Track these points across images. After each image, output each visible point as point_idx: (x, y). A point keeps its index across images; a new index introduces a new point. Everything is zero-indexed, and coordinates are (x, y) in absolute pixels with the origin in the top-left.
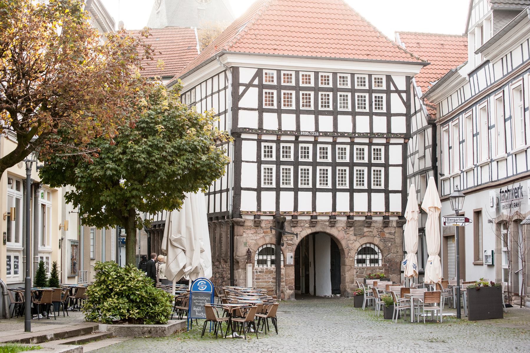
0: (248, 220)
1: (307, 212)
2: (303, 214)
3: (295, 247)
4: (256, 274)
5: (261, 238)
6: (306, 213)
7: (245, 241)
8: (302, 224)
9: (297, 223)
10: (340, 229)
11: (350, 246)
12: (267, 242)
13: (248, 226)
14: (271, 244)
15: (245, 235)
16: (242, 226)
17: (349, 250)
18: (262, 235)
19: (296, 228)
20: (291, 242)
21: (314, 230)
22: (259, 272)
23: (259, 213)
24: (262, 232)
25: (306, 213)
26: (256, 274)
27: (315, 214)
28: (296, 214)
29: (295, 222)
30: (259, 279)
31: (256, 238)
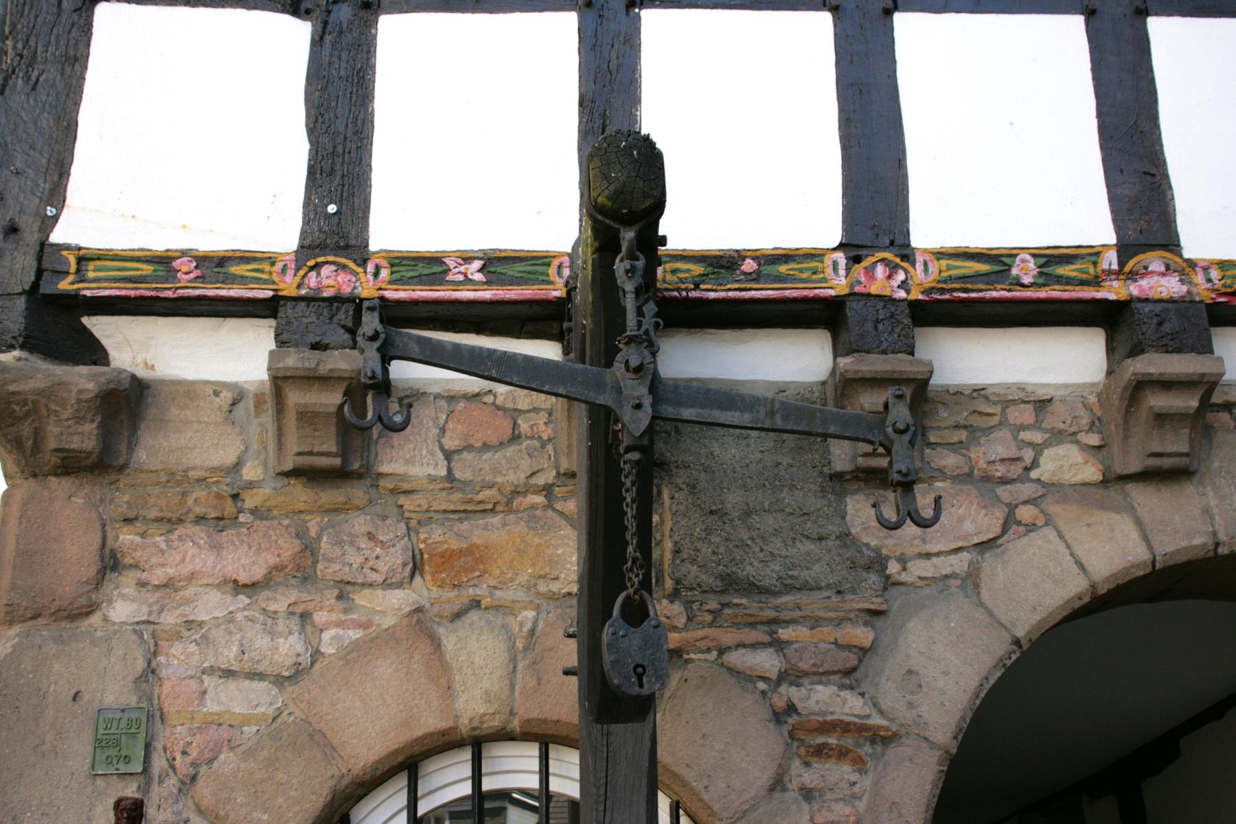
0: (189, 391)
1: (1050, 259)
2: (989, 295)
5: (378, 641)
6: (1026, 270)
7: (115, 692)
9: (917, 434)
12: (473, 705)
13: (178, 479)
14: (546, 739)
15: (123, 608)
16: (99, 467)
18: (390, 605)
20: (851, 706)
23: (330, 279)
24: (394, 559)
25: (1026, 270)
27: (1171, 287)
28: (881, 280)
29: (888, 434)
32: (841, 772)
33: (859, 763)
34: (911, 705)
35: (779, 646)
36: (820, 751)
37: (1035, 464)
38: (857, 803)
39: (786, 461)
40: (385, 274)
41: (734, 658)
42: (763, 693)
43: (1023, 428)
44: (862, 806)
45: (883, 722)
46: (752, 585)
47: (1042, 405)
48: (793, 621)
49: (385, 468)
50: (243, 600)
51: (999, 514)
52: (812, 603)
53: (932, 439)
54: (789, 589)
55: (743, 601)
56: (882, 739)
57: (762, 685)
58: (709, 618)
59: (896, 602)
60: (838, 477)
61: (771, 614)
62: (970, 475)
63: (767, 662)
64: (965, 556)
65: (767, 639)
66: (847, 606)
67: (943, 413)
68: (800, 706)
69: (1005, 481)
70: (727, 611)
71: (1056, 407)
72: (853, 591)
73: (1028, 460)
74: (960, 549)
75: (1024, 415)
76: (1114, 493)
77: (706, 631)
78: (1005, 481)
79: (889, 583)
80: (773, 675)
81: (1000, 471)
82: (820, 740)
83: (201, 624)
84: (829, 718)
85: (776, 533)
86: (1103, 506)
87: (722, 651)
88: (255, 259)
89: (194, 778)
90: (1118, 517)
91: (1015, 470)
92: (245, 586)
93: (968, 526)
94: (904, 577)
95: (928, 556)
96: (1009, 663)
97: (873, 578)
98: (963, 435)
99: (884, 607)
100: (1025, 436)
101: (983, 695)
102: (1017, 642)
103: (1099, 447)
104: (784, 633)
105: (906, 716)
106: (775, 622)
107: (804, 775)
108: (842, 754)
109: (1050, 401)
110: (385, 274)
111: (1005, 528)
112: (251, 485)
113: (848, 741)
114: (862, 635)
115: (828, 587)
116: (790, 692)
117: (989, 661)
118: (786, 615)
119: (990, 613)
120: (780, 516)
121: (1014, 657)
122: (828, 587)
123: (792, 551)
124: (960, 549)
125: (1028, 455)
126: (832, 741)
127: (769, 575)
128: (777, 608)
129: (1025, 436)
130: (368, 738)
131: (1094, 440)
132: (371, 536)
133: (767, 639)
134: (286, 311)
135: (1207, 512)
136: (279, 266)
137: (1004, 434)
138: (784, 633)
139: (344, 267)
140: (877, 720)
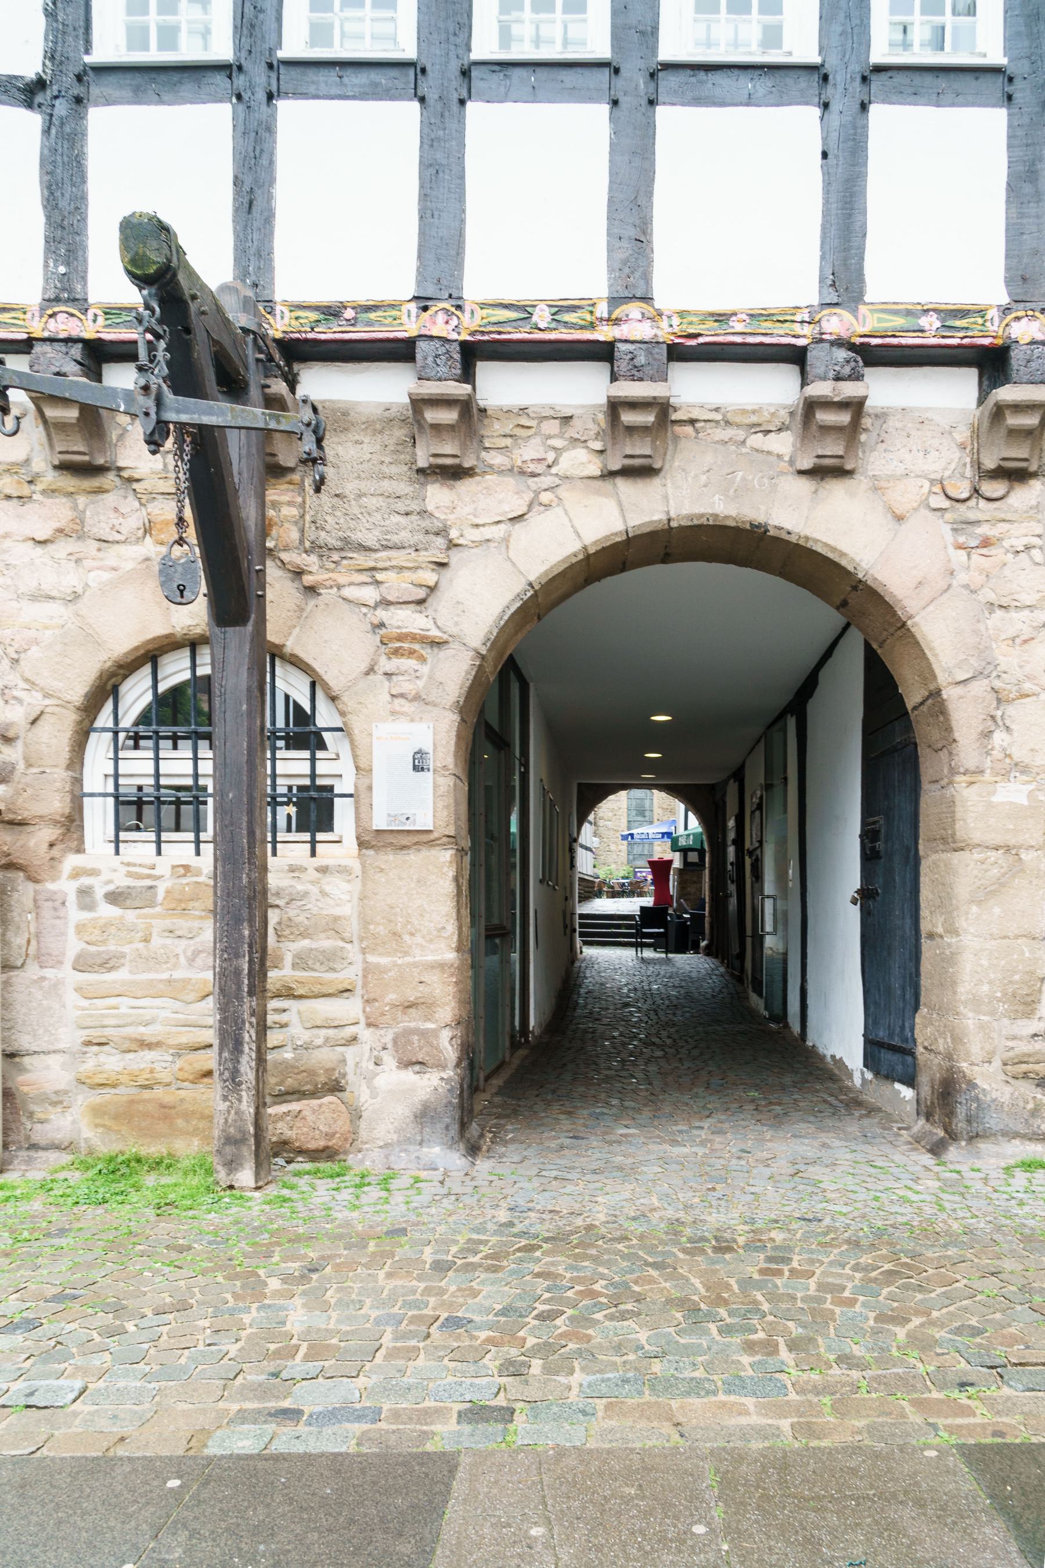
3: (453, 674)
4: (75, 915)
8: (529, 452)
10: (908, 494)
11: (1007, 658)
17: (1000, 698)
19: (465, 486)
21: (645, 507)
22: (115, 898)
26: (75, 915)
30: (107, 964)
31: (70, 579)
32: (409, 663)
33: (422, 659)
34: (456, 624)
35: (378, 583)
36: (396, 652)
37: (555, 462)
38: (418, 682)
39: (387, 460)
40: (101, 320)
41: (347, 592)
42: (365, 614)
43: (549, 437)
44: (420, 684)
45: (438, 634)
46: (360, 545)
47: (567, 419)
48: (386, 569)
49: (120, 464)
50: (40, 550)
51: (528, 496)
52: (400, 558)
53: (487, 445)
54: (386, 547)
55: (355, 555)
56: (436, 644)
57: (364, 610)
58: (333, 566)
59: (455, 557)
60: (421, 471)
61: (372, 564)
62: (511, 470)
63: (369, 594)
64: (502, 526)
65: (369, 580)
66: (420, 559)
67: (497, 426)
68: (387, 623)
69: (534, 475)
70: (345, 562)
71: (575, 422)
72: (426, 549)
73: (550, 461)
74: (499, 522)
75: (552, 427)
76: (607, 485)
77: (331, 575)
78: (534, 475)
79: (452, 545)
80: (372, 603)
81: (532, 467)
82: (398, 644)
83: (15, 567)
84: (404, 631)
85: (378, 509)
86: (598, 493)
87: (339, 587)
88: (13, 309)
89: (17, 661)
90: (606, 500)
91: (539, 468)
92: (40, 542)
93: (506, 508)
94: (461, 541)
95: (477, 526)
96: (525, 598)
97: (440, 542)
98: (508, 441)
99: (445, 561)
100: (552, 442)
101: (506, 618)
102: (531, 585)
103: (602, 452)
104: (379, 576)
105: (454, 631)
106: (374, 569)
107: (386, 664)
108: (411, 653)
109: (571, 417)
110: (101, 320)
111: (530, 506)
112: (38, 475)
113: (417, 647)
114: (429, 577)
115: (410, 546)
116: (382, 614)
117: (510, 596)
118: (380, 565)
119: (514, 564)
120: (380, 499)
121: (529, 594)
122: (410, 546)
123: (387, 523)
124: (499, 522)
125: (551, 456)
126: (406, 645)
127: (370, 539)
128: (376, 560)
129: (552, 442)
130: (123, 642)
131: (598, 445)
132: (116, 510)
133: (369, 580)
134: (38, 348)
135: (666, 498)
136: (29, 316)
137: (537, 441)
138: (379, 576)
139: (72, 315)
140: (434, 633)
